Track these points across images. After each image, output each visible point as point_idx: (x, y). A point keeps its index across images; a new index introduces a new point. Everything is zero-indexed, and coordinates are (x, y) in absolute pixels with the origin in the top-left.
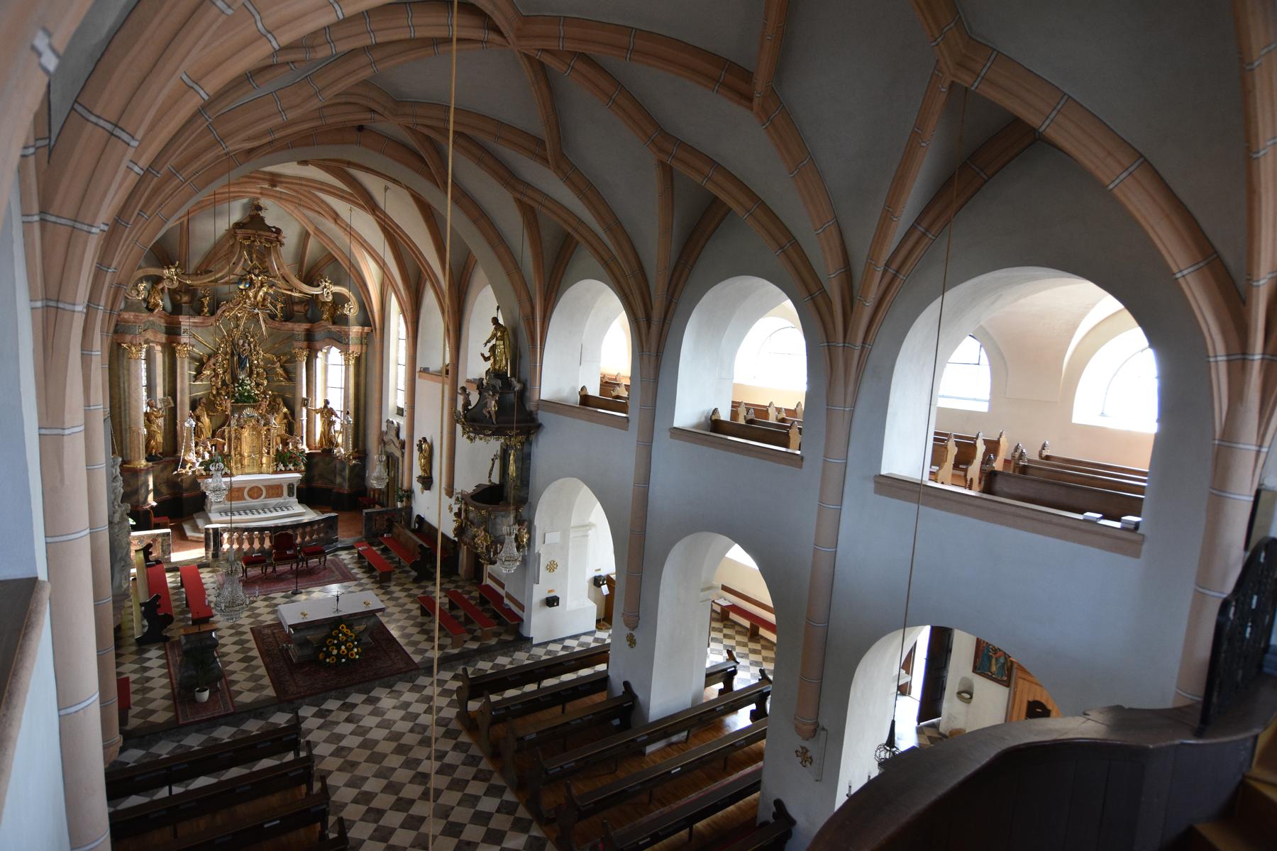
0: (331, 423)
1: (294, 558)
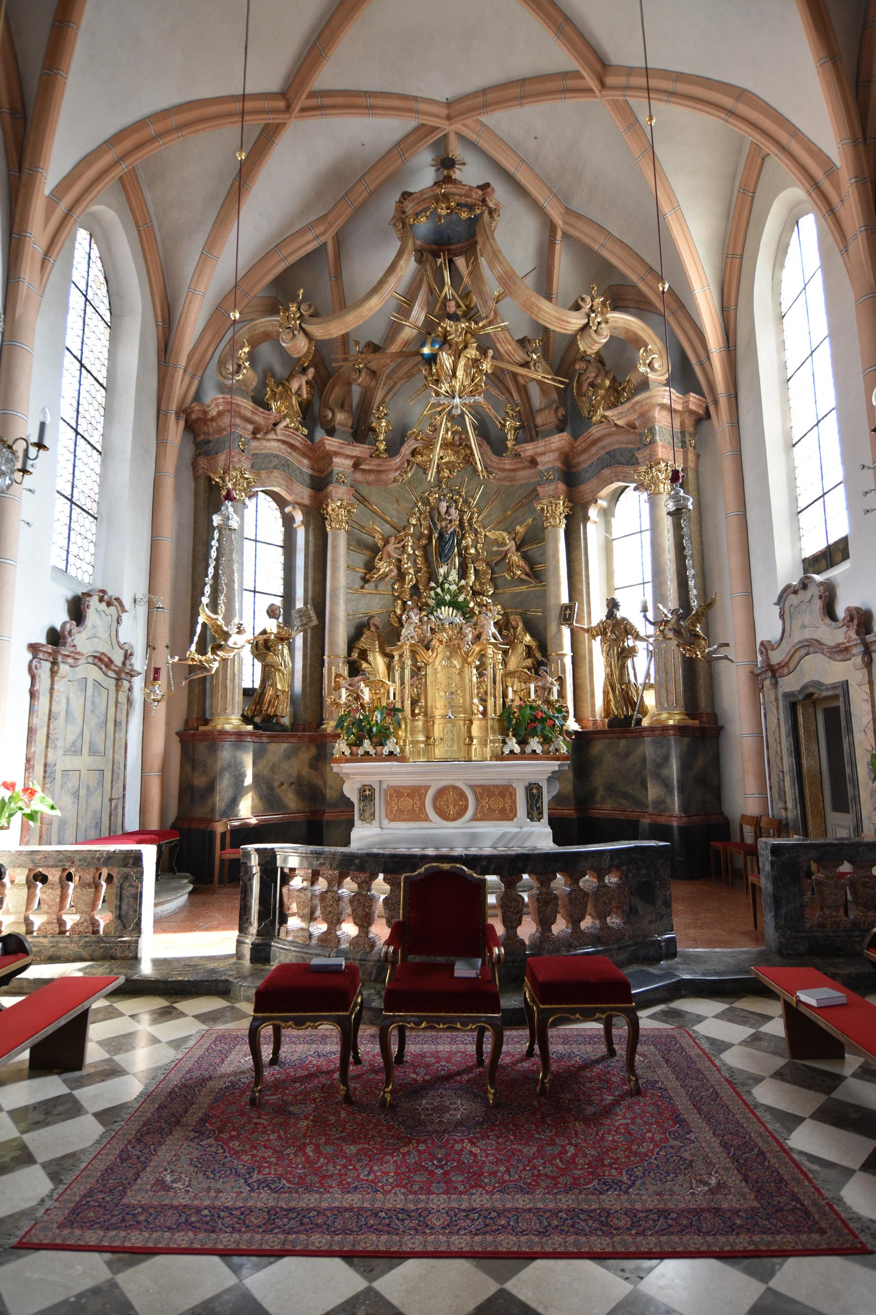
0: (626, 654)
1: (475, 999)
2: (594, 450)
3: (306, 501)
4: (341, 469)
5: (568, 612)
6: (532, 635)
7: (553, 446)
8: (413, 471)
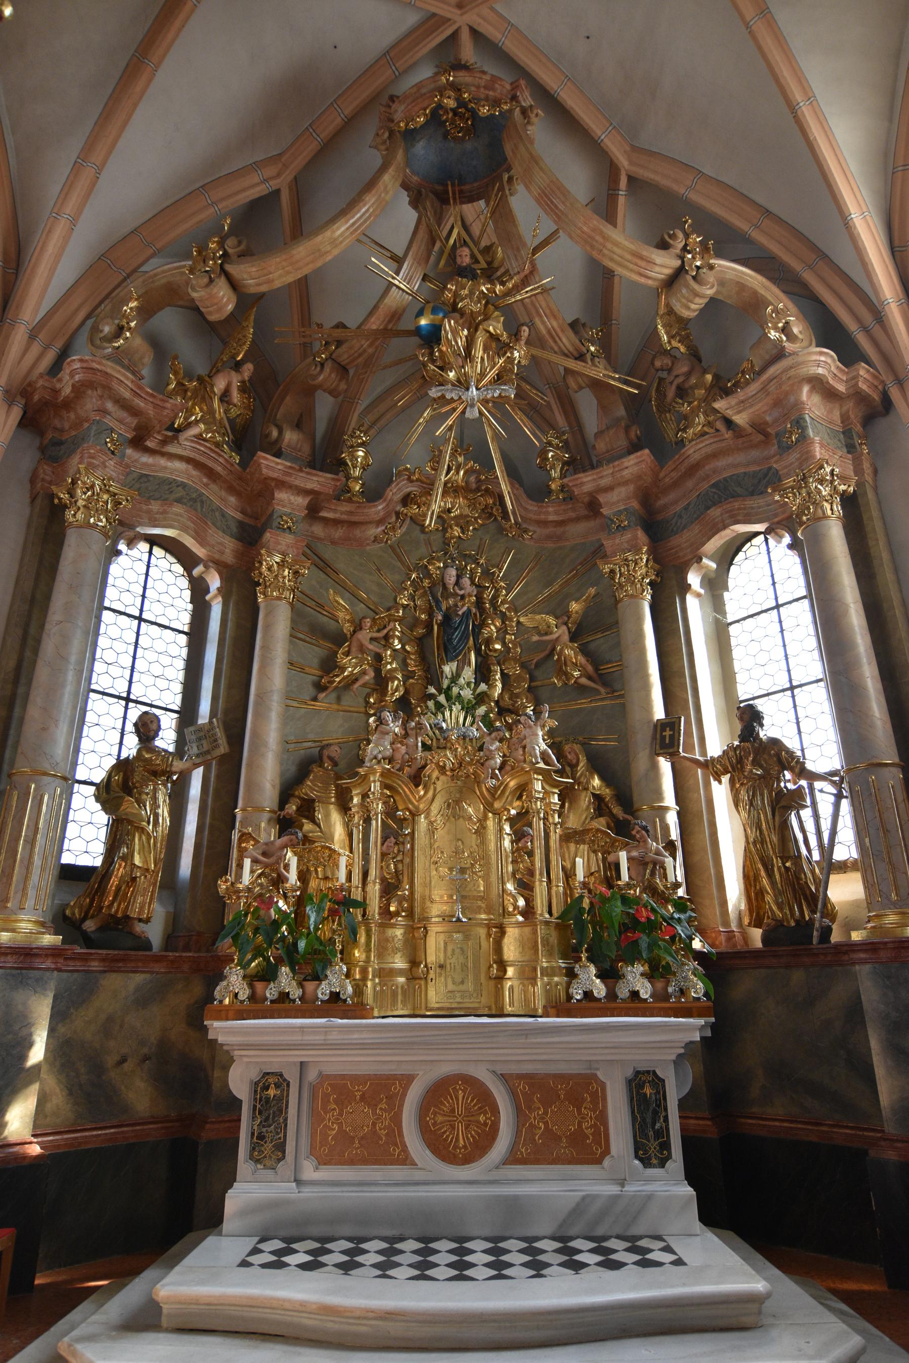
3: (229, 557)
4: (287, 510)
5: (668, 733)
6: (602, 778)
8: (404, 529)
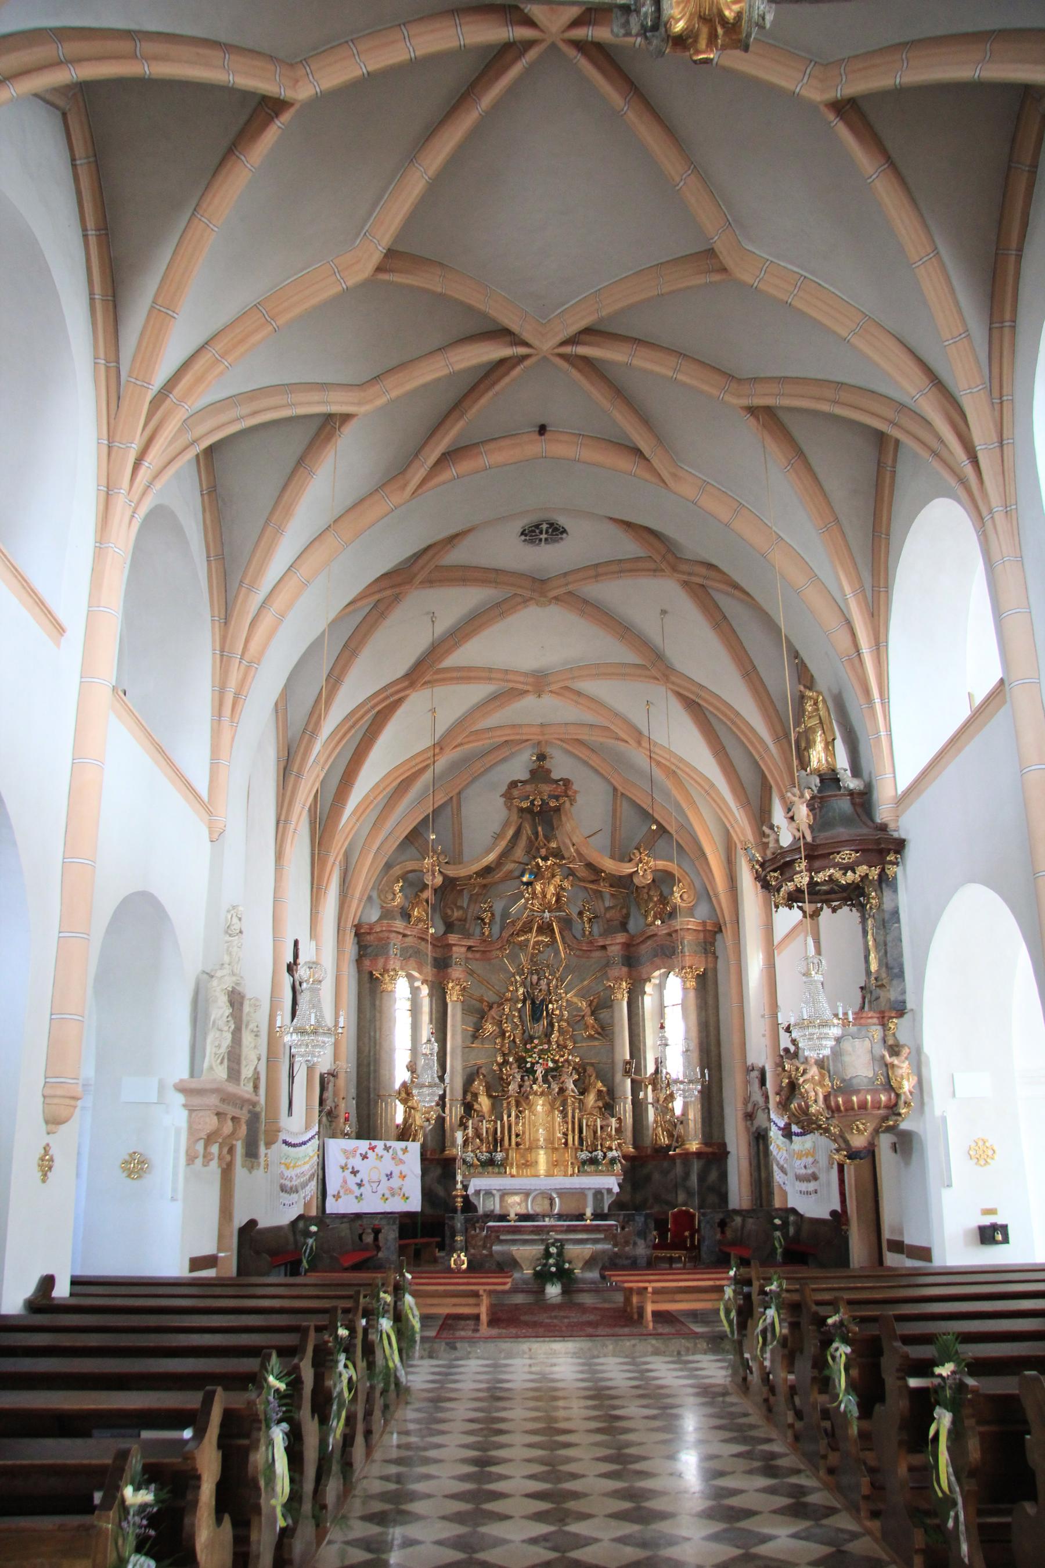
2: (649, 942)
7: (618, 941)
